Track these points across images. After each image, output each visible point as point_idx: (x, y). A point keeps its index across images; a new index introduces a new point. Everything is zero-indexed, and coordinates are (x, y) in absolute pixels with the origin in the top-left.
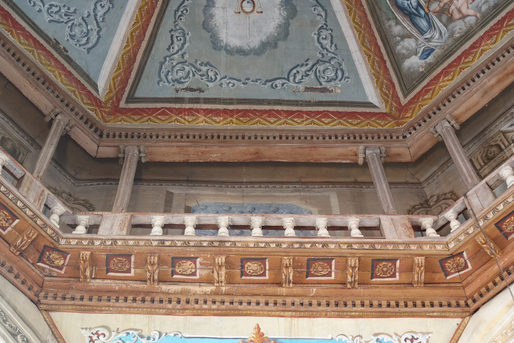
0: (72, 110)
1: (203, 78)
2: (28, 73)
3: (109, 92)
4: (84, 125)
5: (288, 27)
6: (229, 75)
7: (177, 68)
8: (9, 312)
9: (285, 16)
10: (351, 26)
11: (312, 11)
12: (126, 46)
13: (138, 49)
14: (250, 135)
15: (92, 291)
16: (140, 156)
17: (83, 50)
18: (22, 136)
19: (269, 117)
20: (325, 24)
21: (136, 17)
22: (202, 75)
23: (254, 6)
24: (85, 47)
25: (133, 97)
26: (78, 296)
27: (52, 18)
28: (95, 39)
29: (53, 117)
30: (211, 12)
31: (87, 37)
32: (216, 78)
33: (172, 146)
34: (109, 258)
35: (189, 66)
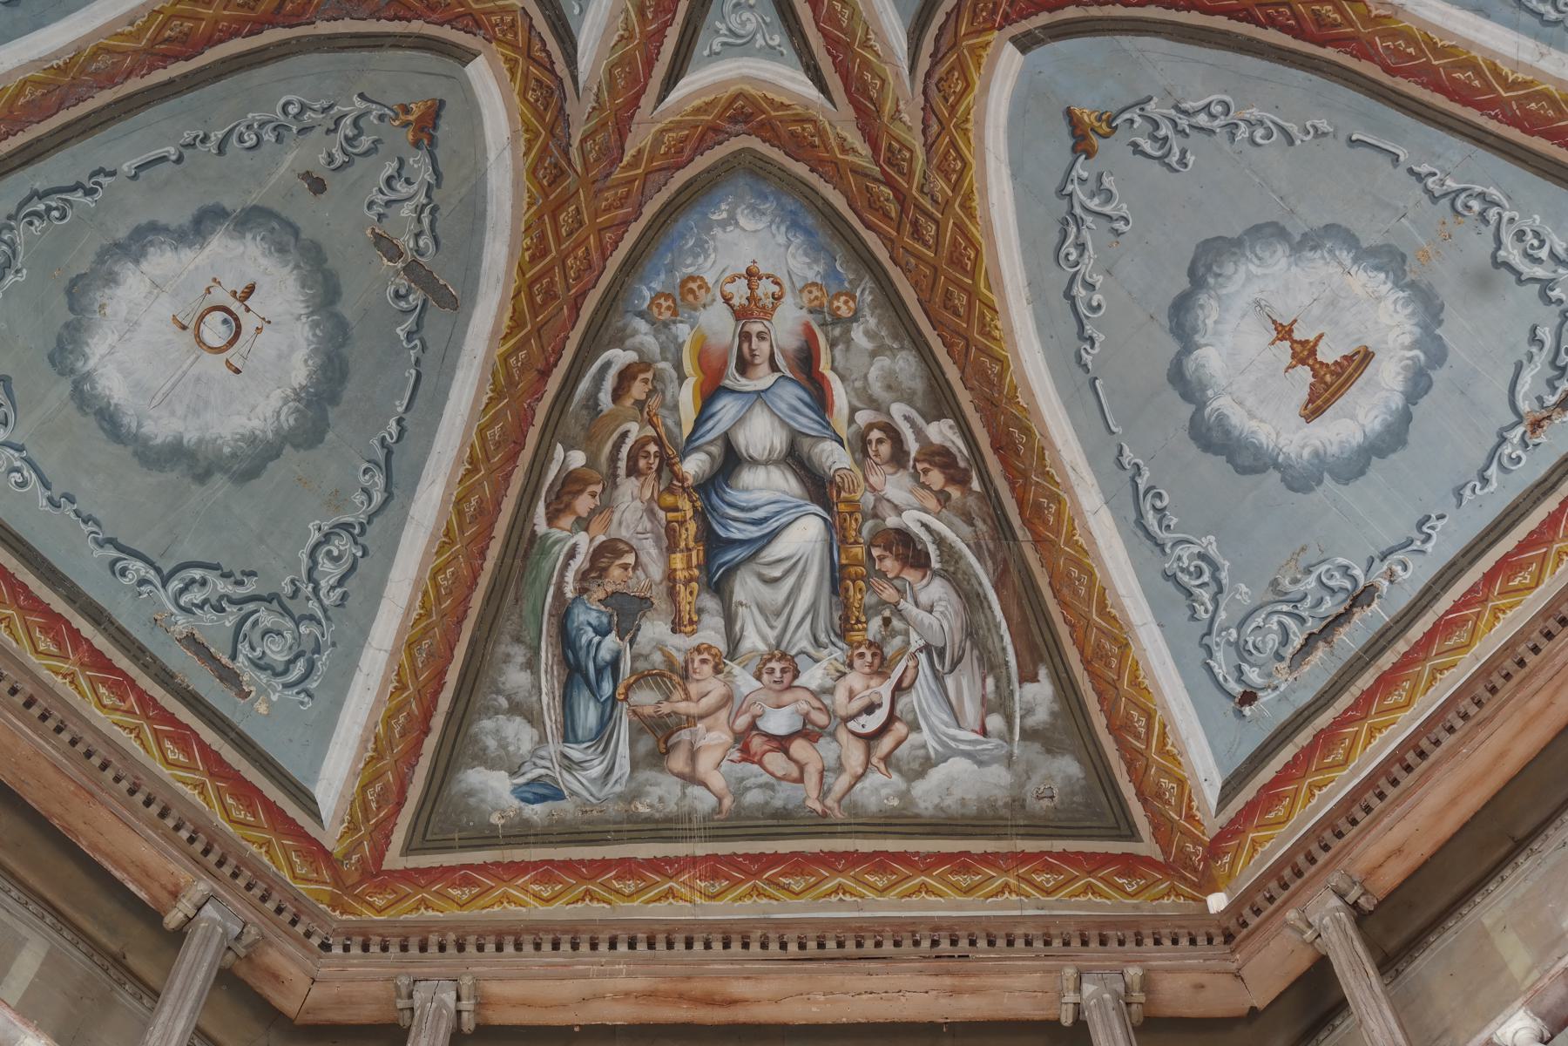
5: (271, 459)
6: (32, 452)
9: (286, 426)
10: (417, 582)
19: (45, 630)
20: (361, 524)
23: (231, 343)
30: (116, 269)
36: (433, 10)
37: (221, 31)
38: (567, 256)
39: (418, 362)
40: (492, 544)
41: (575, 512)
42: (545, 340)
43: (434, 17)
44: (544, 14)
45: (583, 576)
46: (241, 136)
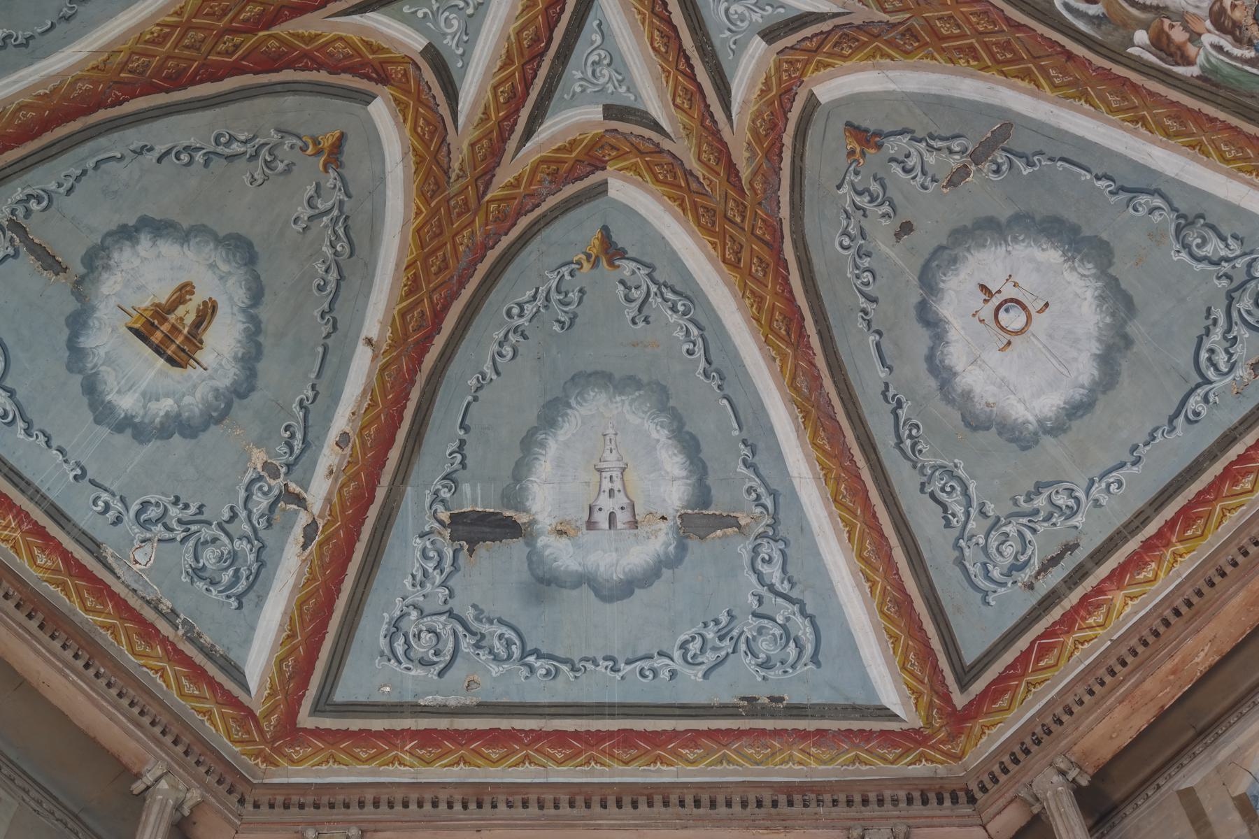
0: (881, 802)
1: (1054, 520)
3: (916, 699)
4: (925, 811)
5: (1118, 285)
6: (1096, 472)
7: (993, 544)
9: (1093, 271)
10: (1229, 175)
11: (1132, 217)
12: (870, 587)
13: (897, 573)
16: (1070, 779)
17: (806, 668)
19: (1235, 483)
20: (1178, 217)
21: (843, 521)
22: (1048, 518)
23: (1024, 307)
24: (804, 660)
25: (967, 670)
27: (704, 667)
28: (809, 630)
30: (959, 391)
31: (792, 641)
32: (1077, 500)
33: (1110, 710)
35: (1010, 522)
36: (776, 125)
37: (783, 291)
38: (976, 30)
39: (1051, 159)
40: (1205, 111)
41: (1185, 43)
42: (1041, 53)
43: (781, 124)
44: (784, 37)
45: (1238, 41)
46: (863, 283)
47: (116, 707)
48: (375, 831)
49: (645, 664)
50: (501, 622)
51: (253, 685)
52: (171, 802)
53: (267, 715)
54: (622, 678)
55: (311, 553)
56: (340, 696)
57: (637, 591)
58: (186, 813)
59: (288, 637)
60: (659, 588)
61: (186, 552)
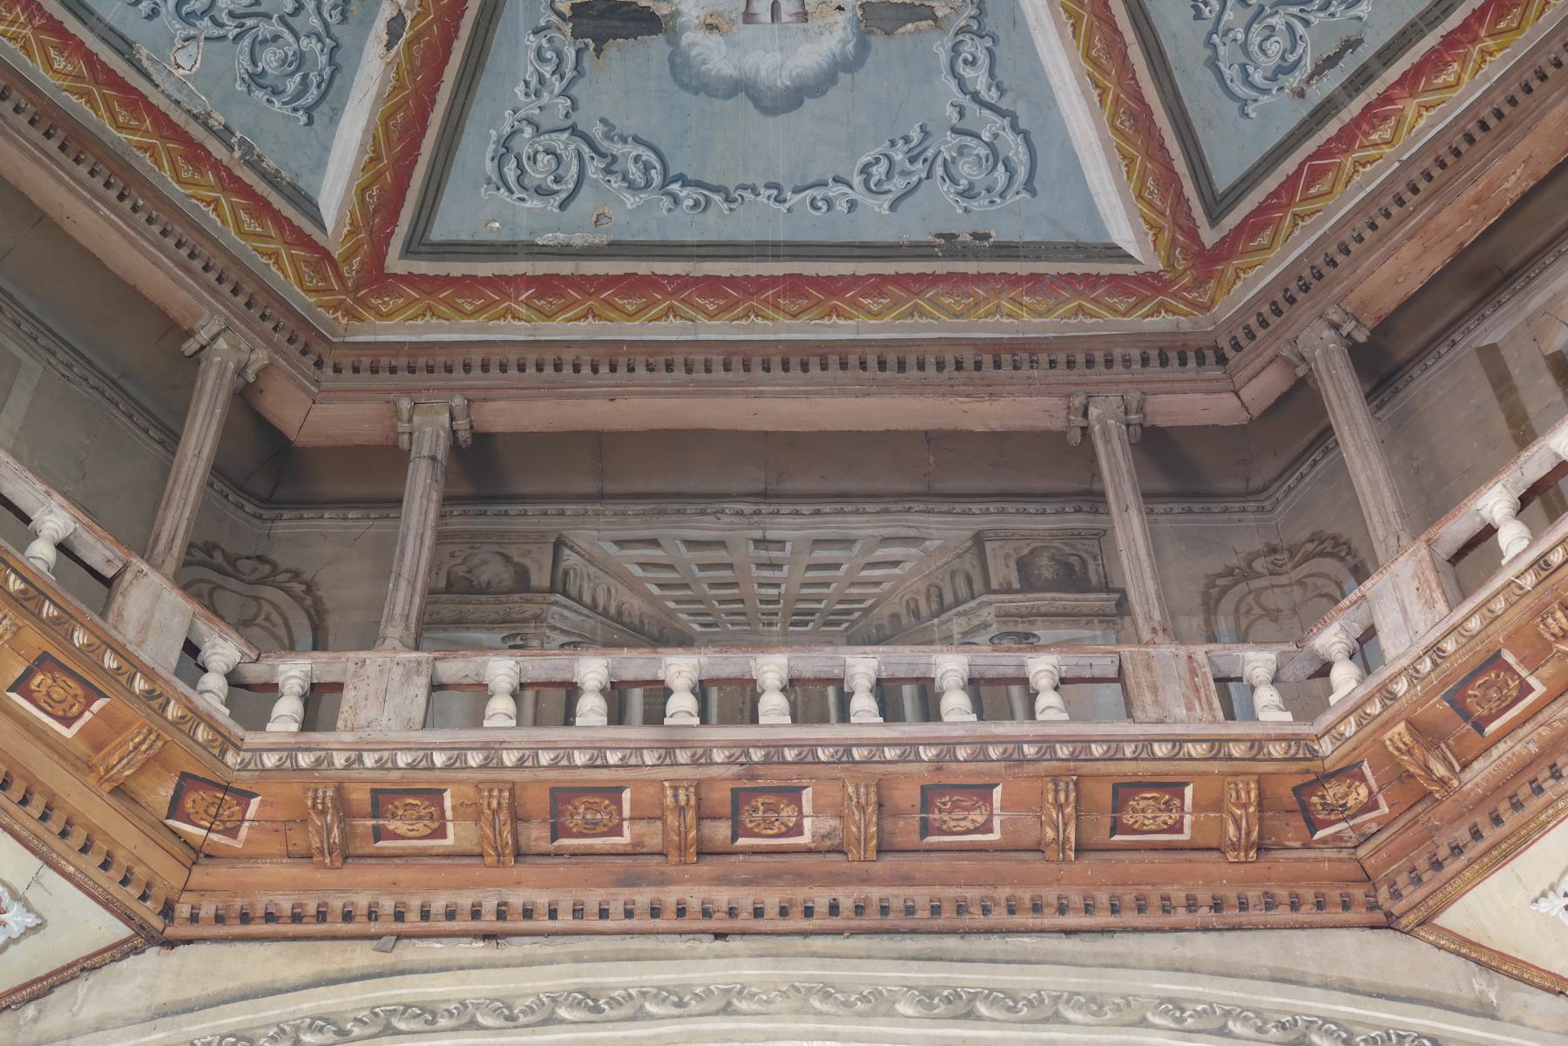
0: (1109, 363)
1: (1332, 9)
2: (946, 373)
3: (1155, 235)
4: (1164, 374)
7: (1255, 40)
8: (1342, 1008)
12: (1100, 95)
13: (1134, 78)
14: (1553, 55)
15: (1482, 799)
16: (1345, 334)
18: (1057, 512)
21: (1066, 11)
24: (1015, 187)
25: (1218, 199)
26: (1463, 834)
27: (891, 197)
28: (1022, 149)
29: (1079, 421)
31: (1000, 163)
33: (1397, 248)
34: (1456, 700)
35: (1277, 12)
47: (159, 247)
48: (485, 400)
49: (818, 193)
50: (637, 140)
51: (329, 219)
52: (232, 365)
53: (348, 258)
54: (789, 210)
55: (397, 54)
56: (437, 233)
57: (807, 101)
58: (251, 378)
59: (372, 160)
60: (834, 96)
61: (241, 53)
